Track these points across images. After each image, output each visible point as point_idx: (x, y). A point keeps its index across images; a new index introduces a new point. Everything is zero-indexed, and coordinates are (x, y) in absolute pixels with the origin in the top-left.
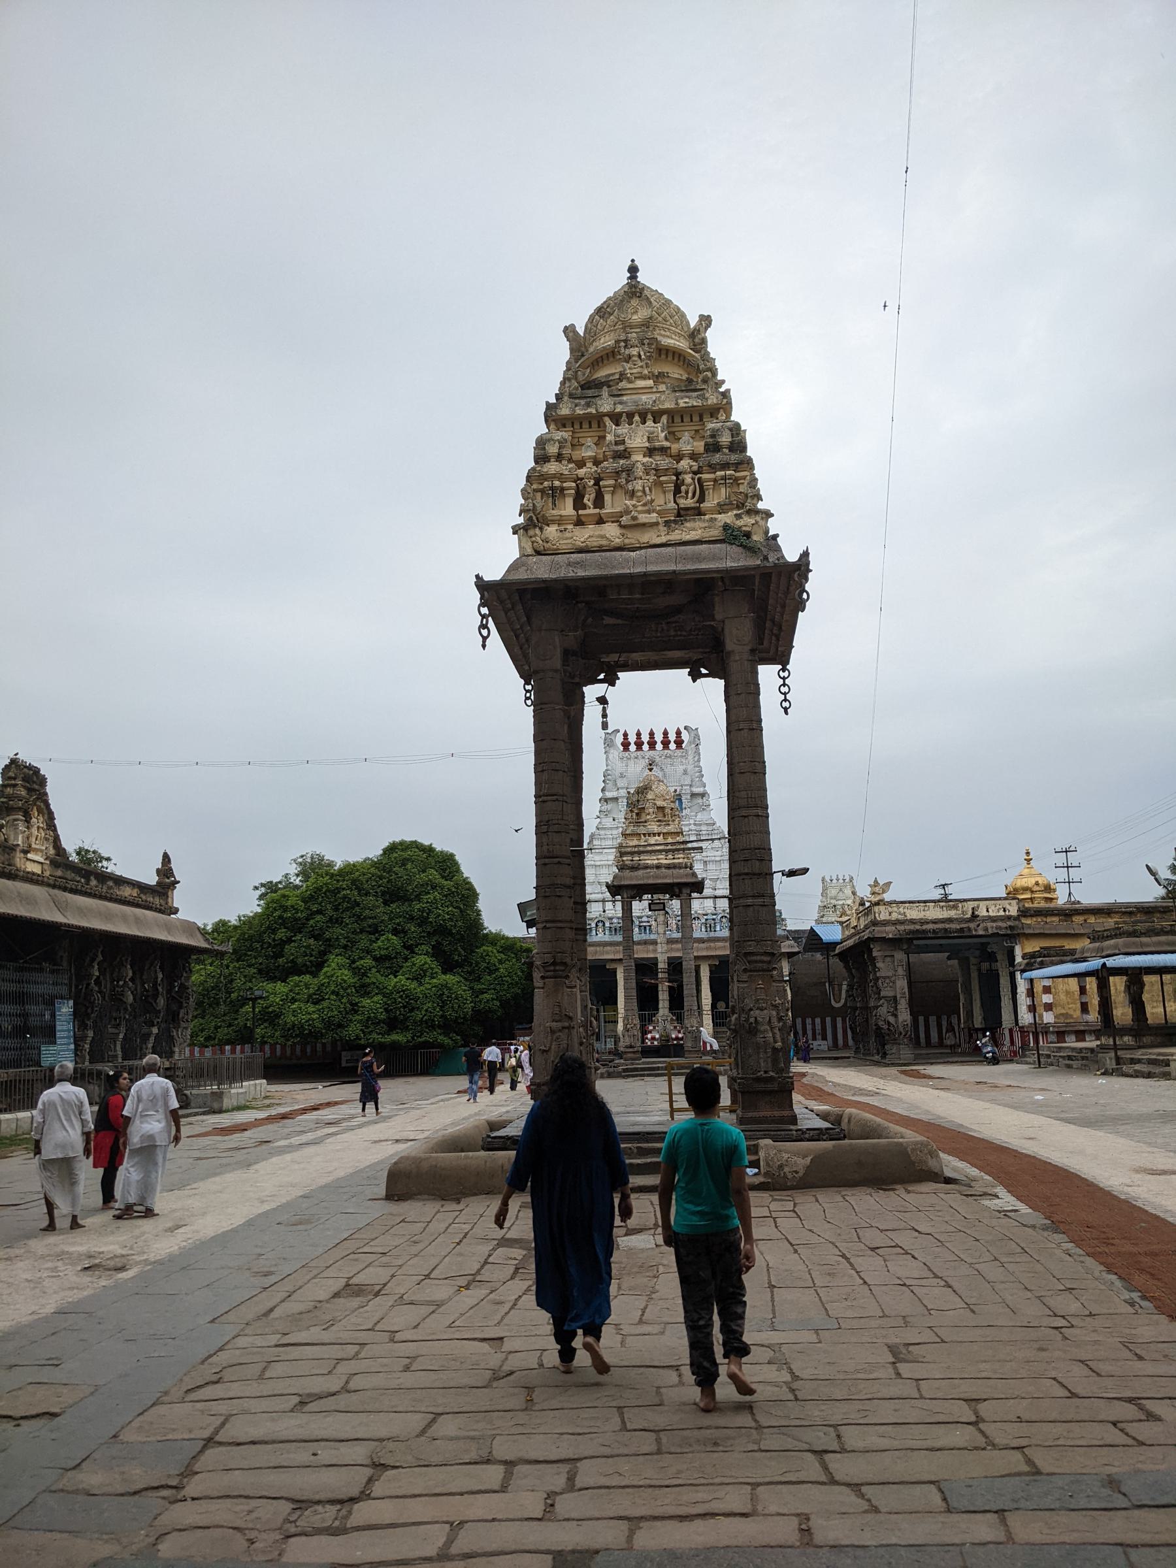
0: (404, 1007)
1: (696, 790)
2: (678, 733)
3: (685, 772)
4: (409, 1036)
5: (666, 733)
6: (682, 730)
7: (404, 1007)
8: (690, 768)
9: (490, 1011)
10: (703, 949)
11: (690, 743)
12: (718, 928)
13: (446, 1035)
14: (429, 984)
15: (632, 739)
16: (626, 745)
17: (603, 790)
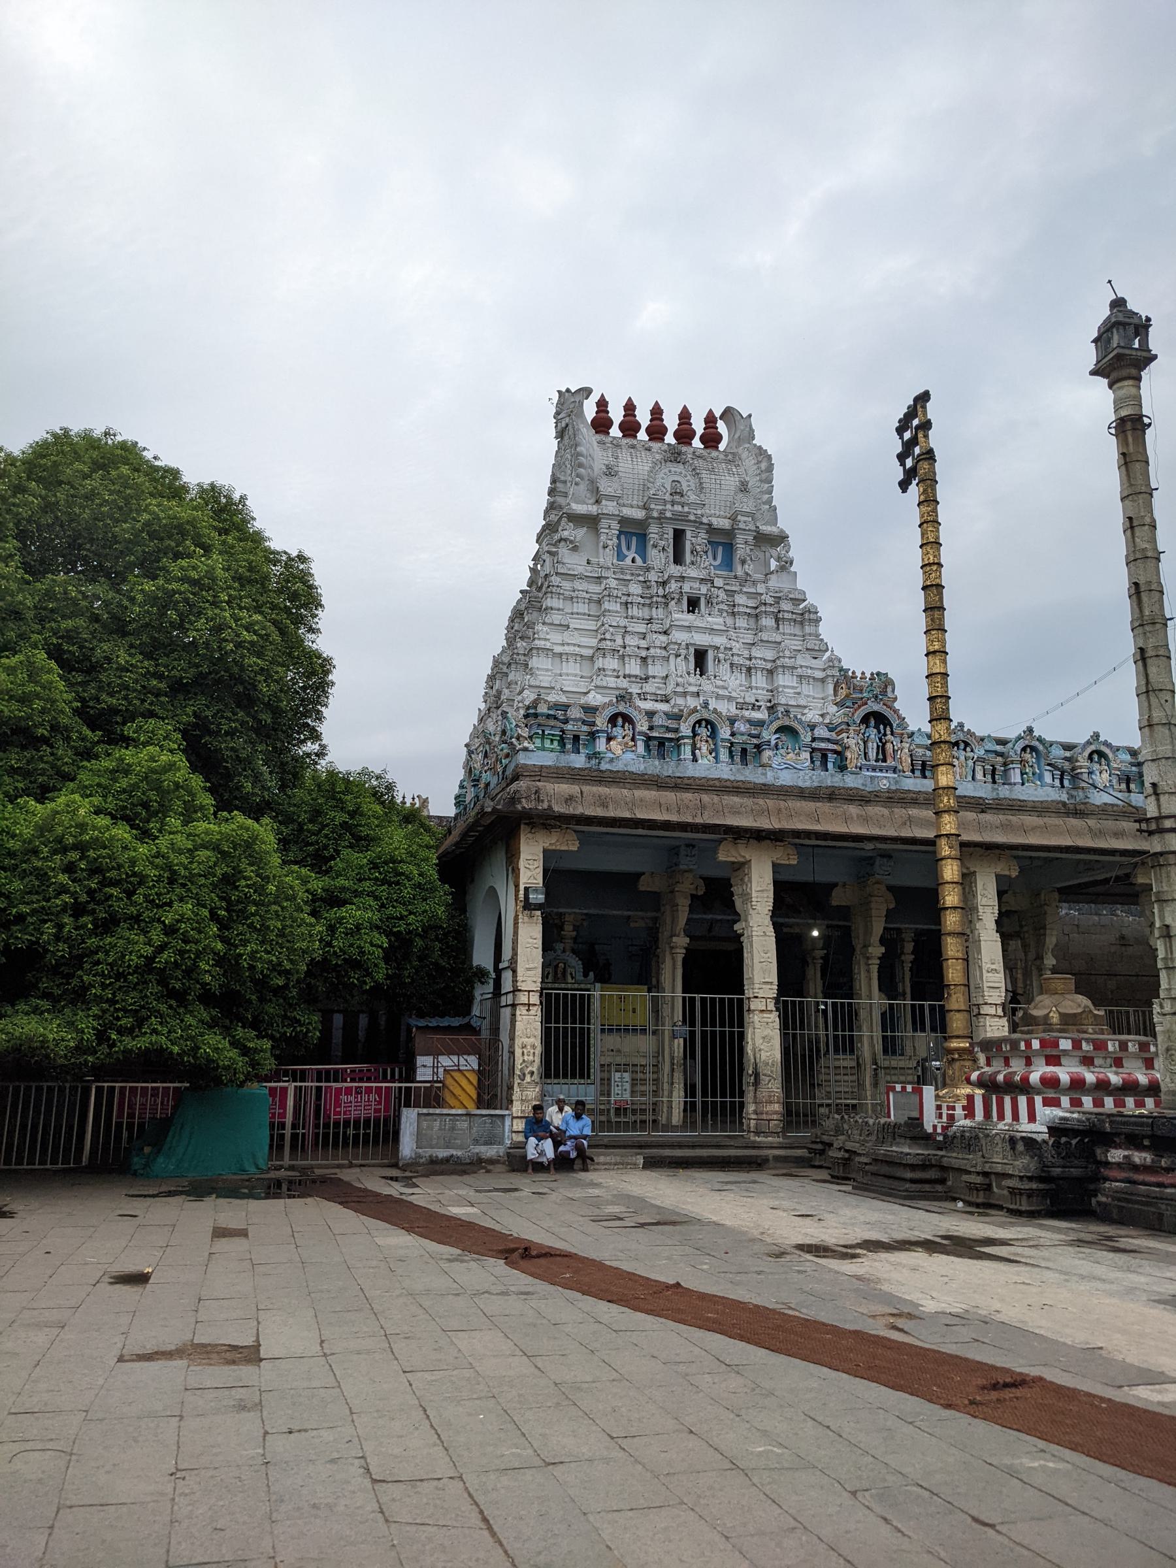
0: (78, 910)
1: (766, 529)
2: (710, 420)
3: (744, 488)
4: (87, 1024)
5: (685, 416)
6: (718, 414)
7: (78, 910)
8: (753, 482)
9: (355, 964)
10: (993, 827)
11: (737, 441)
12: (1016, 776)
13: (227, 1031)
14: (174, 835)
15: (616, 414)
16: (601, 424)
17: (551, 507)
